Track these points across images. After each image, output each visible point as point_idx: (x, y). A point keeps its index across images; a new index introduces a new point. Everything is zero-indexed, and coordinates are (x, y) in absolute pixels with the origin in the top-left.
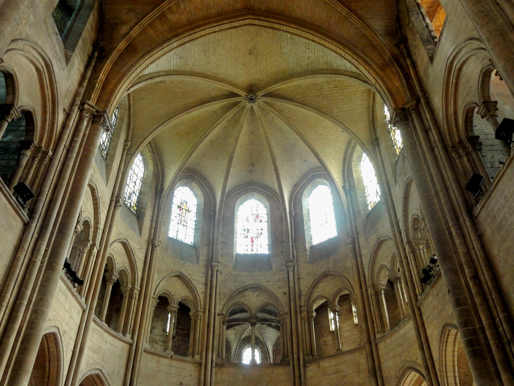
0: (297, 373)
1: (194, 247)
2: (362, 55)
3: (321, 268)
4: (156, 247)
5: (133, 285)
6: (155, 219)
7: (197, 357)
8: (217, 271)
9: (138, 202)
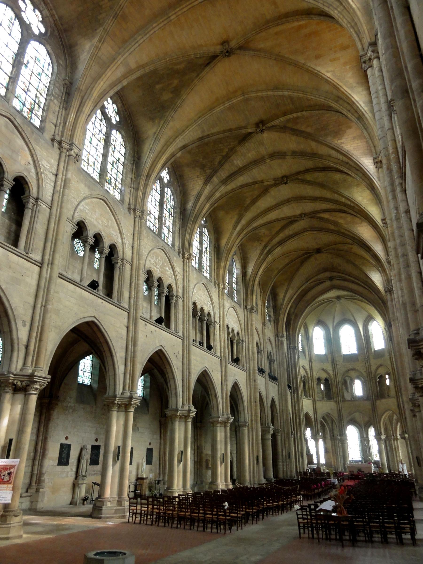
1: (325, 355)
2: (378, 308)
3: (379, 361)
7: (335, 399)
9: (302, 345)
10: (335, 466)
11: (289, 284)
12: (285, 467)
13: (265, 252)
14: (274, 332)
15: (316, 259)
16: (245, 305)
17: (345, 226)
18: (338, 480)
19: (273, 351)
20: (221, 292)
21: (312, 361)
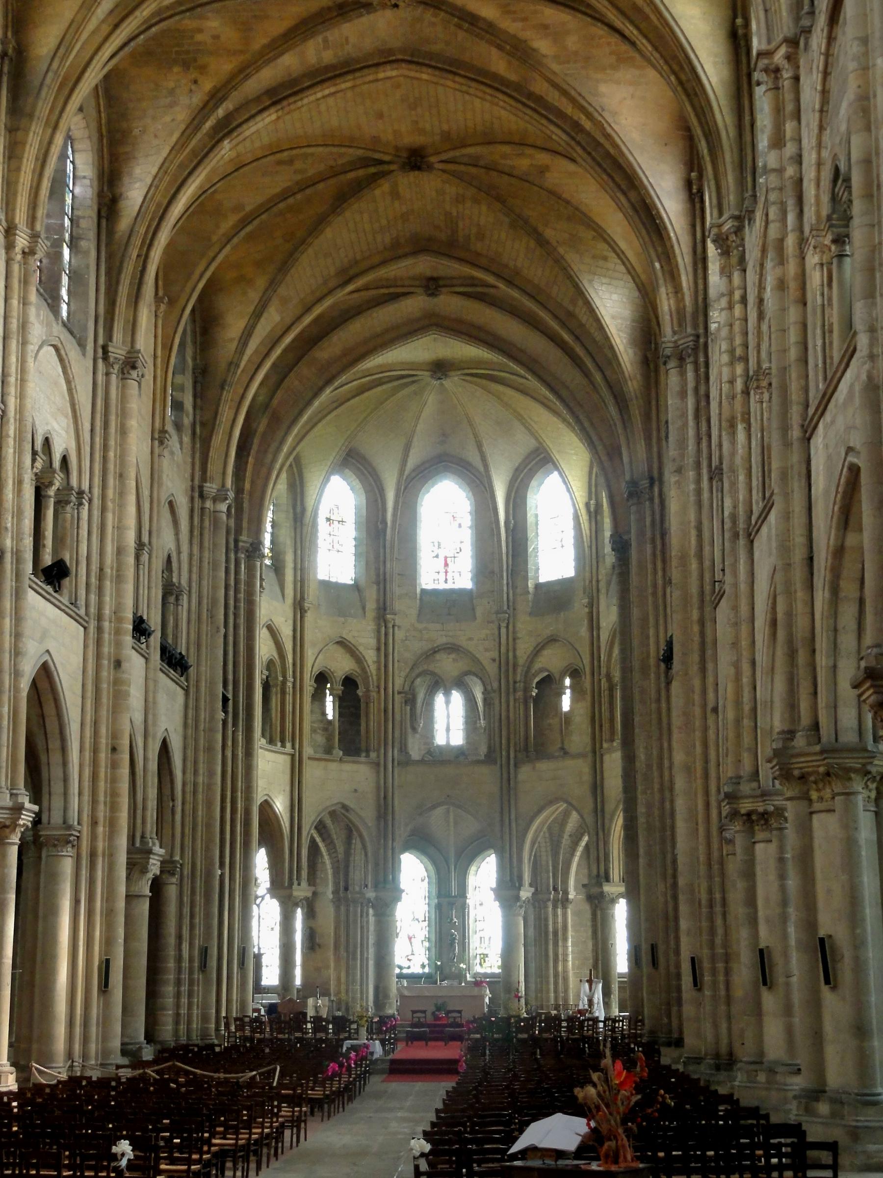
0: (505, 776)
1: (356, 587)
2: (586, 424)
3: (549, 625)
4: (306, 612)
5: (284, 677)
6: (299, 566)
7: (373, 755)
8: (393, 626)
10: (338, 993)
11: (273, 285)
12: (184, 1000)
13: (208, 124)
14: (188, 475)
15: (395, 194)
16: (101, 341)
17: (555, 67)
18: (383, 1043)
19: (179, 553)
20: (16, 268)
21: (306, 605)
